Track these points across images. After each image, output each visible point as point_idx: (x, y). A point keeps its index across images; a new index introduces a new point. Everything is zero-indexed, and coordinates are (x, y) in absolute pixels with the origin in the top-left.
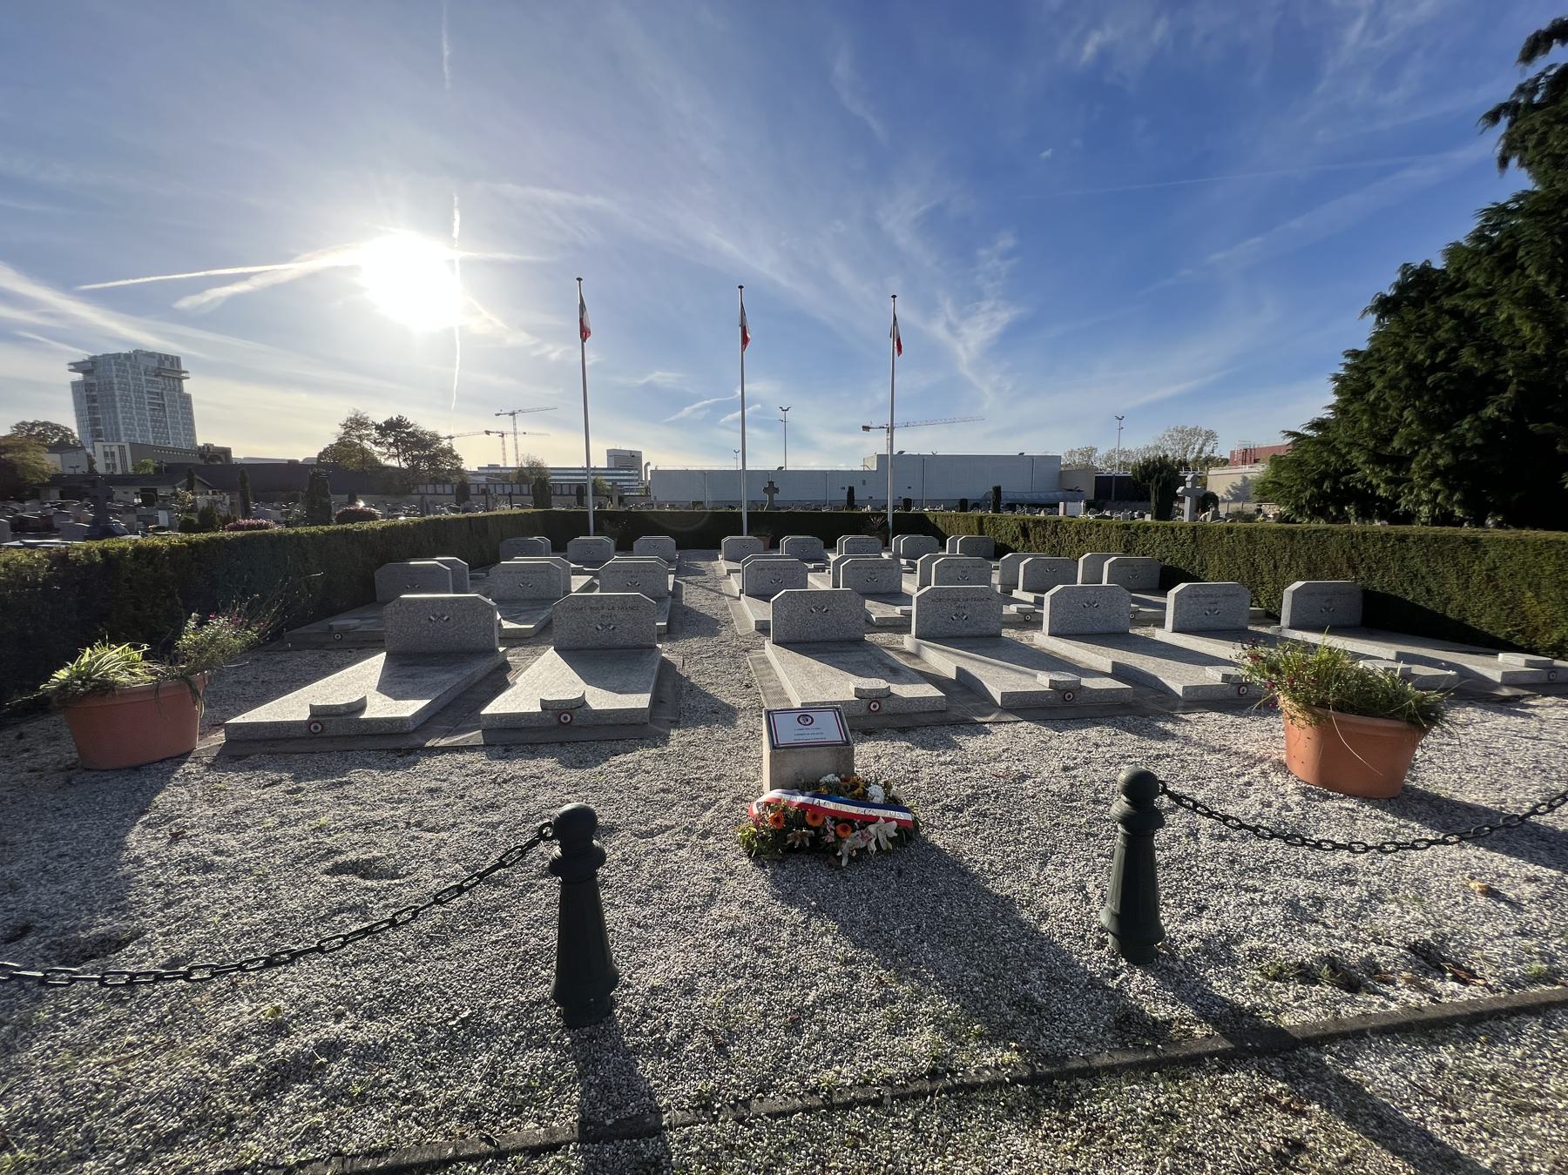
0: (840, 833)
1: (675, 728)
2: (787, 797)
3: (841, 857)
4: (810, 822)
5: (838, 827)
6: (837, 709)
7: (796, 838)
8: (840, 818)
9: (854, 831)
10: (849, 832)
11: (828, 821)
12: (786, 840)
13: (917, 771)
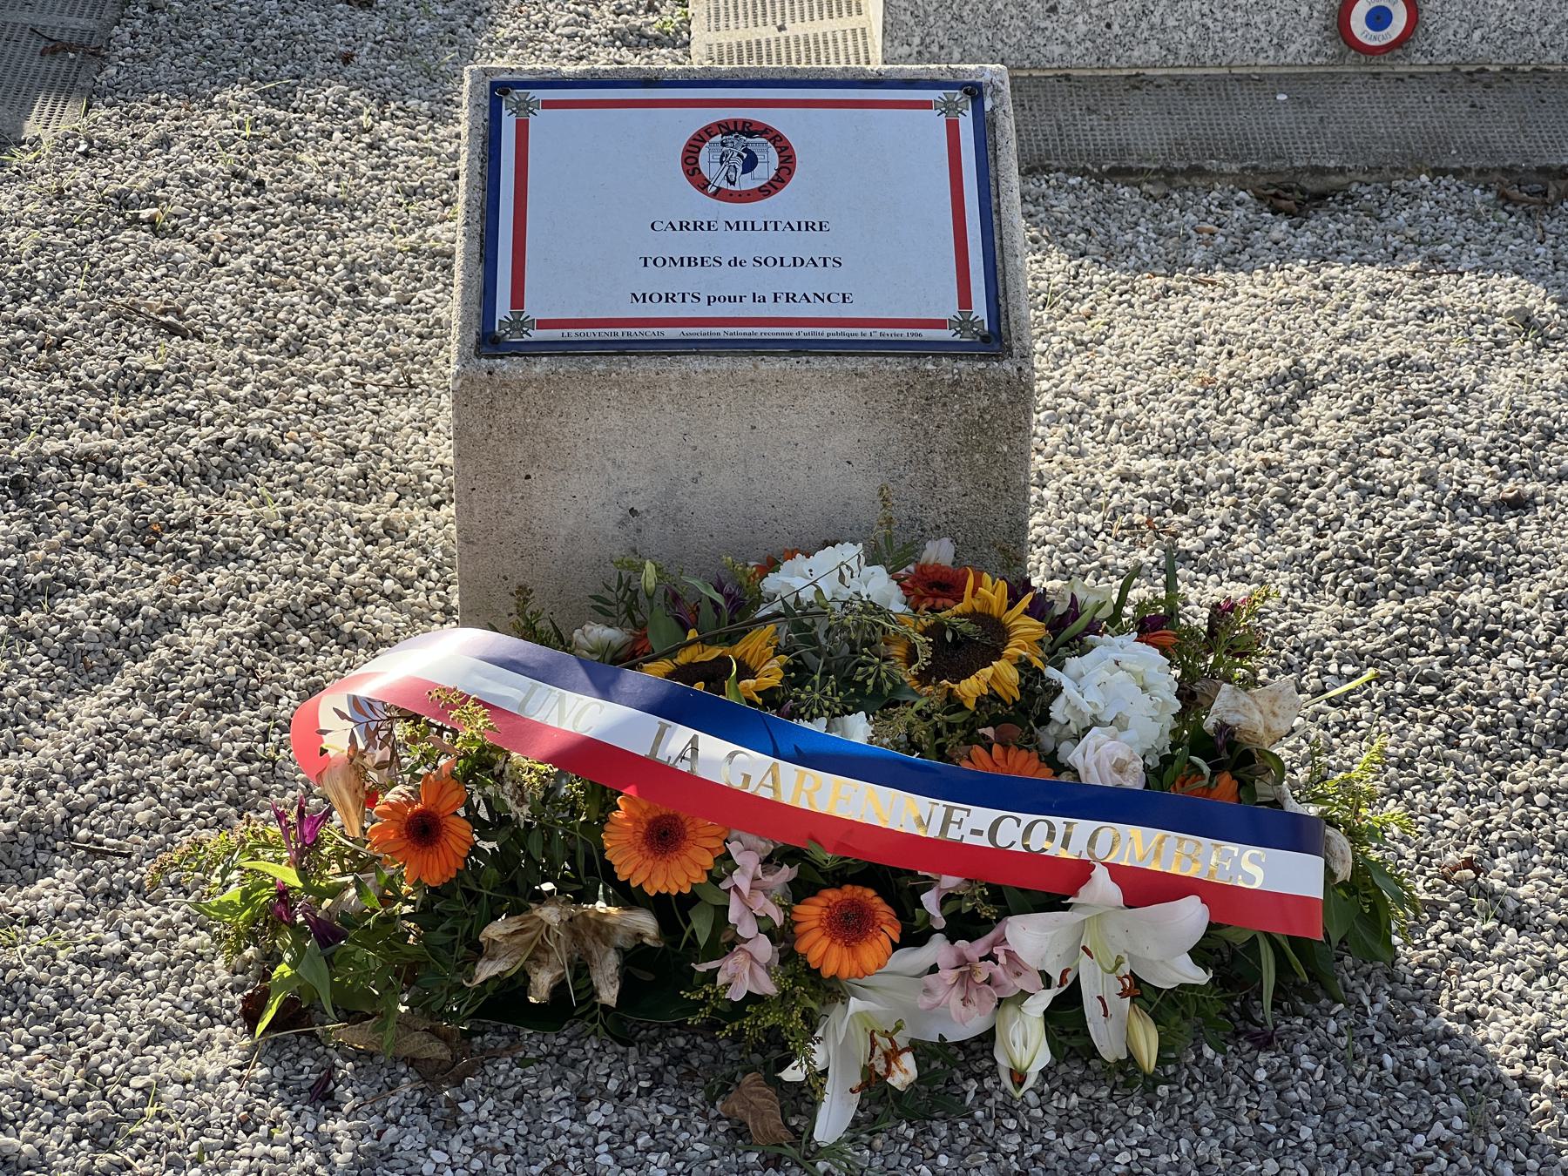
0: (820, 950)
1: (65, 88)
2: (509, 689)
3: (804, 1099)
4: (629, 864)
5: (811, 912)
6: (975, 91)
7: (539, 952)
8: (825, 857)
9: (914, 936)
10: (871, 952)
11: (747, 862)
12: (478, 951)
13: (1520, 504)
